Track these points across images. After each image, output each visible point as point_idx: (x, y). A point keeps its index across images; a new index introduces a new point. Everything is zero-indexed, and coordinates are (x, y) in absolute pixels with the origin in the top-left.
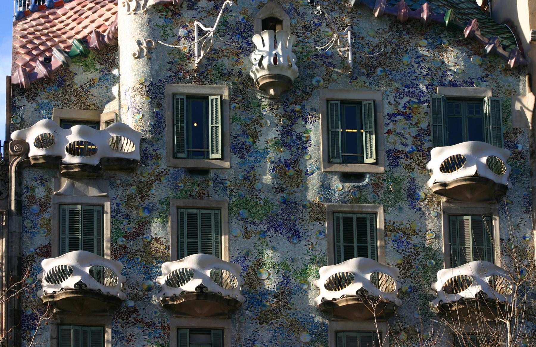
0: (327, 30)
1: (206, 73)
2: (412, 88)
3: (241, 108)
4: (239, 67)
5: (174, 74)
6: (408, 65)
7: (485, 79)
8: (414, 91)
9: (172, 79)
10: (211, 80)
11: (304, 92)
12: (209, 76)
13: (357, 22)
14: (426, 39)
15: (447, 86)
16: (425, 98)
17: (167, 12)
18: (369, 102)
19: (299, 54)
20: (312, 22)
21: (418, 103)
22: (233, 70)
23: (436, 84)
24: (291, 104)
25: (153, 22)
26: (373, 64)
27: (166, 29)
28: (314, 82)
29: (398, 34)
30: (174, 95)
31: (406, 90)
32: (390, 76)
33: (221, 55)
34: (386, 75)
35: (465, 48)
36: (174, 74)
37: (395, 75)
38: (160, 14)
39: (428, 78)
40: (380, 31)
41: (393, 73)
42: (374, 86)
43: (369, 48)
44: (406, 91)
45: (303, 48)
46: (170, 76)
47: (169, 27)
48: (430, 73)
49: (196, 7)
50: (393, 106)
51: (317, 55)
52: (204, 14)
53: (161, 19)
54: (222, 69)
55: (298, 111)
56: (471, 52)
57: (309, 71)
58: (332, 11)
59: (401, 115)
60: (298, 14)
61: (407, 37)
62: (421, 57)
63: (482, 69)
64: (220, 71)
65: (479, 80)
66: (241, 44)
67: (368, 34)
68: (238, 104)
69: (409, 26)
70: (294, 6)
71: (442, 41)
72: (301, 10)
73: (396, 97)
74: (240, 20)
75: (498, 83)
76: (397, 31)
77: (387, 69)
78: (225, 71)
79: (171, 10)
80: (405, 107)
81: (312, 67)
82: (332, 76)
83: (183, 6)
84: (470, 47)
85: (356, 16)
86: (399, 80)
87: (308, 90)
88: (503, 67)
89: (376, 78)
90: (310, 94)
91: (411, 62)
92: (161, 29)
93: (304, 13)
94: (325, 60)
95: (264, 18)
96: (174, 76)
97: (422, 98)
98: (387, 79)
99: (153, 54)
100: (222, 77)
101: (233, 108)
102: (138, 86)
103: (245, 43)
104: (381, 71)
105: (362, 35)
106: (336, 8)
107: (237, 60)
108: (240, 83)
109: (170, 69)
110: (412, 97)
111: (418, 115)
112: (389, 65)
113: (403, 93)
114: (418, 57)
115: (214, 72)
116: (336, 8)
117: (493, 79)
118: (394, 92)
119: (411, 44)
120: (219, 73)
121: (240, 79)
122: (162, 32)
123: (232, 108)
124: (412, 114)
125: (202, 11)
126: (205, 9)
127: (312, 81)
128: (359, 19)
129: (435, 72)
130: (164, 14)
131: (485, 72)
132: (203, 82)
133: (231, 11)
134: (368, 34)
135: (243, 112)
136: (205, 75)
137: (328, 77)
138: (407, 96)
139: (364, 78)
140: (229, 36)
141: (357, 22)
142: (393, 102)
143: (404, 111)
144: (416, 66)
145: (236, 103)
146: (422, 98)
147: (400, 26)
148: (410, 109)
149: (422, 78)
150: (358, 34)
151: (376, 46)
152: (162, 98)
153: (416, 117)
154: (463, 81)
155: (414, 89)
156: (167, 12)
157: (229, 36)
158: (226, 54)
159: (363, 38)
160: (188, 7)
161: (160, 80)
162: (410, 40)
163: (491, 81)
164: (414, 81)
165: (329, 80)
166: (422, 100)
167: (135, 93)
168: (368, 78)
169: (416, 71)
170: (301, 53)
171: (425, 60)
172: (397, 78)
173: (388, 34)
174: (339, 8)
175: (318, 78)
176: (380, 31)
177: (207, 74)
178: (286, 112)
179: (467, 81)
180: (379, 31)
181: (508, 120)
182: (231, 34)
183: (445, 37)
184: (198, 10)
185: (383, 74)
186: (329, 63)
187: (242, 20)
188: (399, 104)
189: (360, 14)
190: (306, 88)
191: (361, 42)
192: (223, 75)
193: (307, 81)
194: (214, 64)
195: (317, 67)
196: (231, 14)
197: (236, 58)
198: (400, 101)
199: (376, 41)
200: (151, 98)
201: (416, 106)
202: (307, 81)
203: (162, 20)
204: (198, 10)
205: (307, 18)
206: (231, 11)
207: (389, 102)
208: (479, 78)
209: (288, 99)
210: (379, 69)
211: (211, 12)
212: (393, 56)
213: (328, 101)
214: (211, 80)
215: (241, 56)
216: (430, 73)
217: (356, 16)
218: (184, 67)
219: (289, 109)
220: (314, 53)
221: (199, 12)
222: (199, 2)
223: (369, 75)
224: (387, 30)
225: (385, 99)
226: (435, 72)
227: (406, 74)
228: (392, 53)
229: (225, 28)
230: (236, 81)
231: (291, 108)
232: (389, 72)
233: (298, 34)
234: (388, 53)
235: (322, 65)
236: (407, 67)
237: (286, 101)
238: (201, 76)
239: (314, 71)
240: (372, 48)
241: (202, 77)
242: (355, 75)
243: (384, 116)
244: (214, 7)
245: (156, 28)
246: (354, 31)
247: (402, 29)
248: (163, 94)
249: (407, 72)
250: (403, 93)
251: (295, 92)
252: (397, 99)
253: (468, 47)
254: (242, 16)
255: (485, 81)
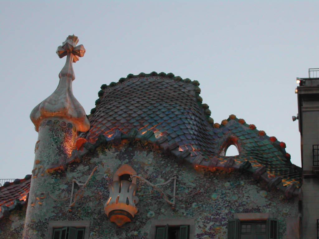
0: (161, 180)
1: (77, 213)
2: (216, 215)
3: (97, 235)
4: (99, 208)
5: (56, 215)
6: (215, 200)
7: (268, 206)
8: (218, 218)
9: (54, 219)
10: (79, 217)
11: (141, 222)
12: (78, 215)
13: (182, 173)
14: (229, 182)
15: (242, 212)
16: (226, 222)
17: (57, 175)
18: (184, 227)
19: (141, 197)
20: (152, 175)
21: (220, 225)
22: (95, 210)
23: (233, 212)
24: (131, 231)
25: (47, 182)
26: (191, 200)
27: (55, 185)
28: (148, 215)
29: (210, 179)
30: (54, 228)
31: (212, 217)
32: (202, 208)
33: (88, 200)
34: (199, 208)
35: (255, 186)
36: (56, 215)
37: (206, 207)
38: (52, 176)
39: (228, 208)
40: (198, 178)
41: (204, 206)
42: (189, 216)
43: (188, 190)
44: (212, 218)
45: (144, 193)
46: (53, 216)
47: (57, 184)
48: (230, 204)
49: (76, 170)
50: (201, 229)
51: (152, 197)
52: (80, 175)
53: (53, 179)
54: (88, 210)
55: (136, 236)
56: (259, 188)
57: (147, 208)
58: (166, 167)
59: (207, 235)
60: (144, 171)
61: (216, 181)
62: (224, 194)
63: (267, 200)
64: (86, 211)
65: (265, 208)
66: (103, 192)
67: (189, 181)
68: (96, 232)
69: (218, 174)
70: (142, 166)
71: (240, 182)
72: (146, 168)
73: (204, 222)
74: (104, 177)
75: (277, 209)
76: (210, 178)
77: (200, 203)
78: (90, 211)
79: (60, 173)
80: (210, 229)
81: (149, 205)
82: (161, 210)
83: (68, 170)
84: (259, 185)
85: (181, 169)
86: (207, 210)
87: (144, 221)
88: (282, 197)
89: (191, 210)
90: (145, 224)
91: (218, 198)
92: (52, 186)
93: (148, 170)
94: (158, 200)
95: (120, 175)
96: (56, 216)
97: (223, 222)
98: (199, 211)
99: (44, 202)
100: (87, 215)
101: (92, 235)
102: (31, 223)
103: (106, 192)
104: (195, 205)
105: (184, 182)
106: (169, 165)
107: (99, 203)
108: (99, 218)
109: (53, 212)
110: (216, 222)
111: (219, 234)
112: (202, 201)
113: (210, 220)
114: (222, 194)
115: (82, 211)
116: (169, 165)
117: (274, 206)
118: (203, 219)
119: (219, 186)
120: (85, 212)
121: (99, 216)
122: (52, 187)
123: (91, 235)
124: (215, 234)
125: (79, 173)
126: (82, 171)
127: (147, 214)
128: (183, 171)
129: (233, 204)
130: (55, 176)
131: (269, 202)
132: (74, 219)
133: (99, 171)
134: (189, 181)
135: (98, 237)
136: (76, 214)
137: (158, 211)
138: (212, 221)
139: (183, 211)
140: (95, 188)
141: (182, 173)
142: (202, 226)
143: (210, 232)
144: (220, 200)
145: (94, 232)
146: (223, 222)
147: (212, 174)
148: (214, 230)
149: (224, 209)
150: (182, 181)
151: (195, 188)
152: (46, 231)
153: (218, 236)
154: (253, 208)
155: (218, 216)
156: (57, 175)
157: (95, 188)
158: (91, 200)
159: (185, 184)
160: (70, 170)
161: (46, 219)
162: (218, 183)
163: (273, 208)
164: (217, 211)
165: (159, 213)
166: (223, 224)
167: (29, 228)
168: (186, 210)
169: (221, 204)
170: (143, 196)
171: (227, 196)
172: (207, 209)
173: (203, 180)
174: (171, 165)
175: (151, 212)
176: (198, 178)
177: (77, 213)
178: (127, 236)
179: (255, 209)
180: (197, 178)
181: (284, 234)
182: (96, 186)
183: (242, 179)
184: (77, 172)
185: (197, 207)
186: (160, 201)
187: (106, 177)
188: (206, 227)
189: (184, 168)
190: (143, 219)
191: (184, 186)
192: (88, 213)
193: (144, 215)
194: (83, 207)
195: (152, 205)
196: (99, 173)
197: (97, 202)
198: (207, 225)
199: (194, 185)
200: (38, 231)
201: (218, 228)
202: (144, 215)
203: (53, 180)
204: (77, 172)
205: (149, 173)
206: (99, 171)
207: (199, 226)
208: (264, 206)
209: (129, 228)
210: (194, 205)
211: (85, 173)
212: (205, 195)
213: (157, 227)
214: (79, 217)
215: (101, 201)
216: (230, 204)
217: (181, 169)
218: (63, 209)
219: (129, 235)
220: (151, 196)
221: (78, 173)
222: (78, 167)
223: (186, 209)
224: (202, 177)
225: (197, 224)
226: (233, 204)
227: (213, 206)
228: (205, 193)
229: (93, 183)
230: (96, 217)
231: (131, 234)
232: (201, 206)
233: (142, 184)
234: (201, 193)
235: (155, 203)
236: (214, 201)
237: (128, 229)
238: (73, 215)
239: (150, 208)
240: (190, 190)
241: (73, 216)
242: (177, 209)
243: (195, 236)
244: (88, 169)
245: (48, 185)
246: (179, 179)
247: (213, 176)
248: (47, 228)
249: (214, 205)
250: (210, 220)
251: (135, 222)
252: (205, 224)
253: (257, 186)
254: (106, 174)
255: (269, 208)
